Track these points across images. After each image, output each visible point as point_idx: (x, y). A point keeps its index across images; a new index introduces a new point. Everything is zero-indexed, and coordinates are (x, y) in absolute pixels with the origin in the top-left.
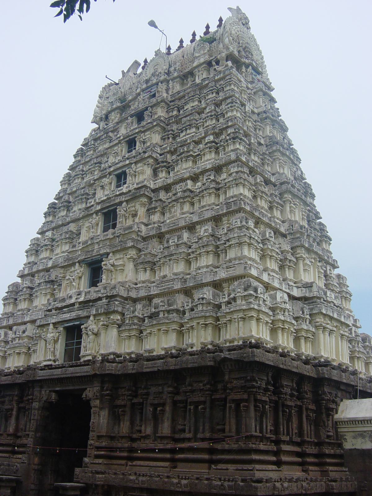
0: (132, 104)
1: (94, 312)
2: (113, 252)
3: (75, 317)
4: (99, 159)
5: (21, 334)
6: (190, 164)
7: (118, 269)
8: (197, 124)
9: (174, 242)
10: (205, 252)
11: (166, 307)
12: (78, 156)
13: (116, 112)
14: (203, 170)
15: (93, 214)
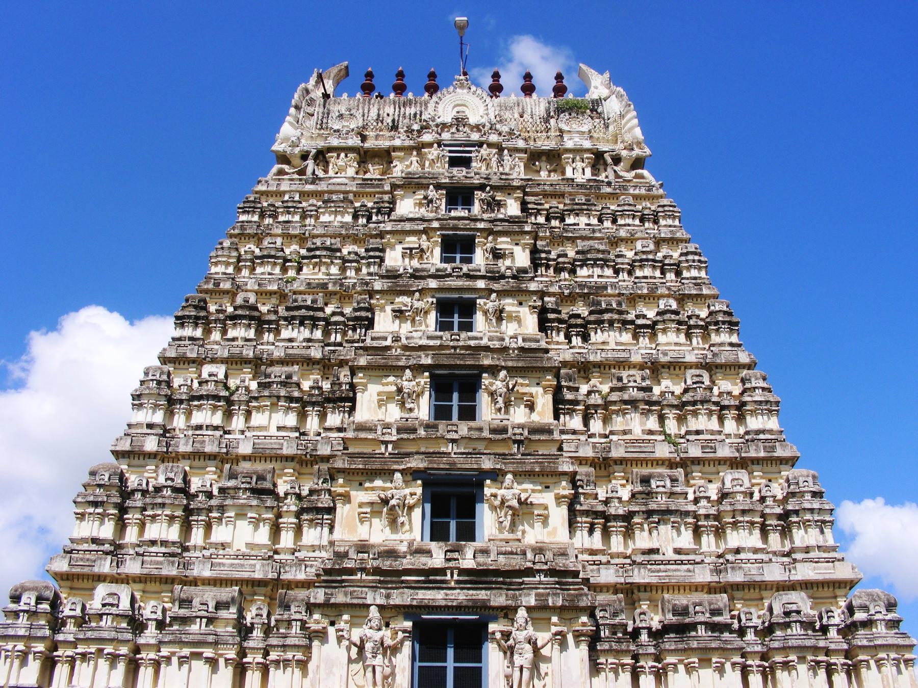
0: (398, 157)
1: (531, 600)
2: (515, 474)
3: (465, 603)
4: (337, 242)
5: (210, 609)
6: (626, 337)
7: (536, 512)
8: (617, 264)
9: (664, 487)
10: (747, 522)
11: (708, 615)
12: (254, 212)
13: (351, 155)
14: (672, 360)
15: (403, 368)
